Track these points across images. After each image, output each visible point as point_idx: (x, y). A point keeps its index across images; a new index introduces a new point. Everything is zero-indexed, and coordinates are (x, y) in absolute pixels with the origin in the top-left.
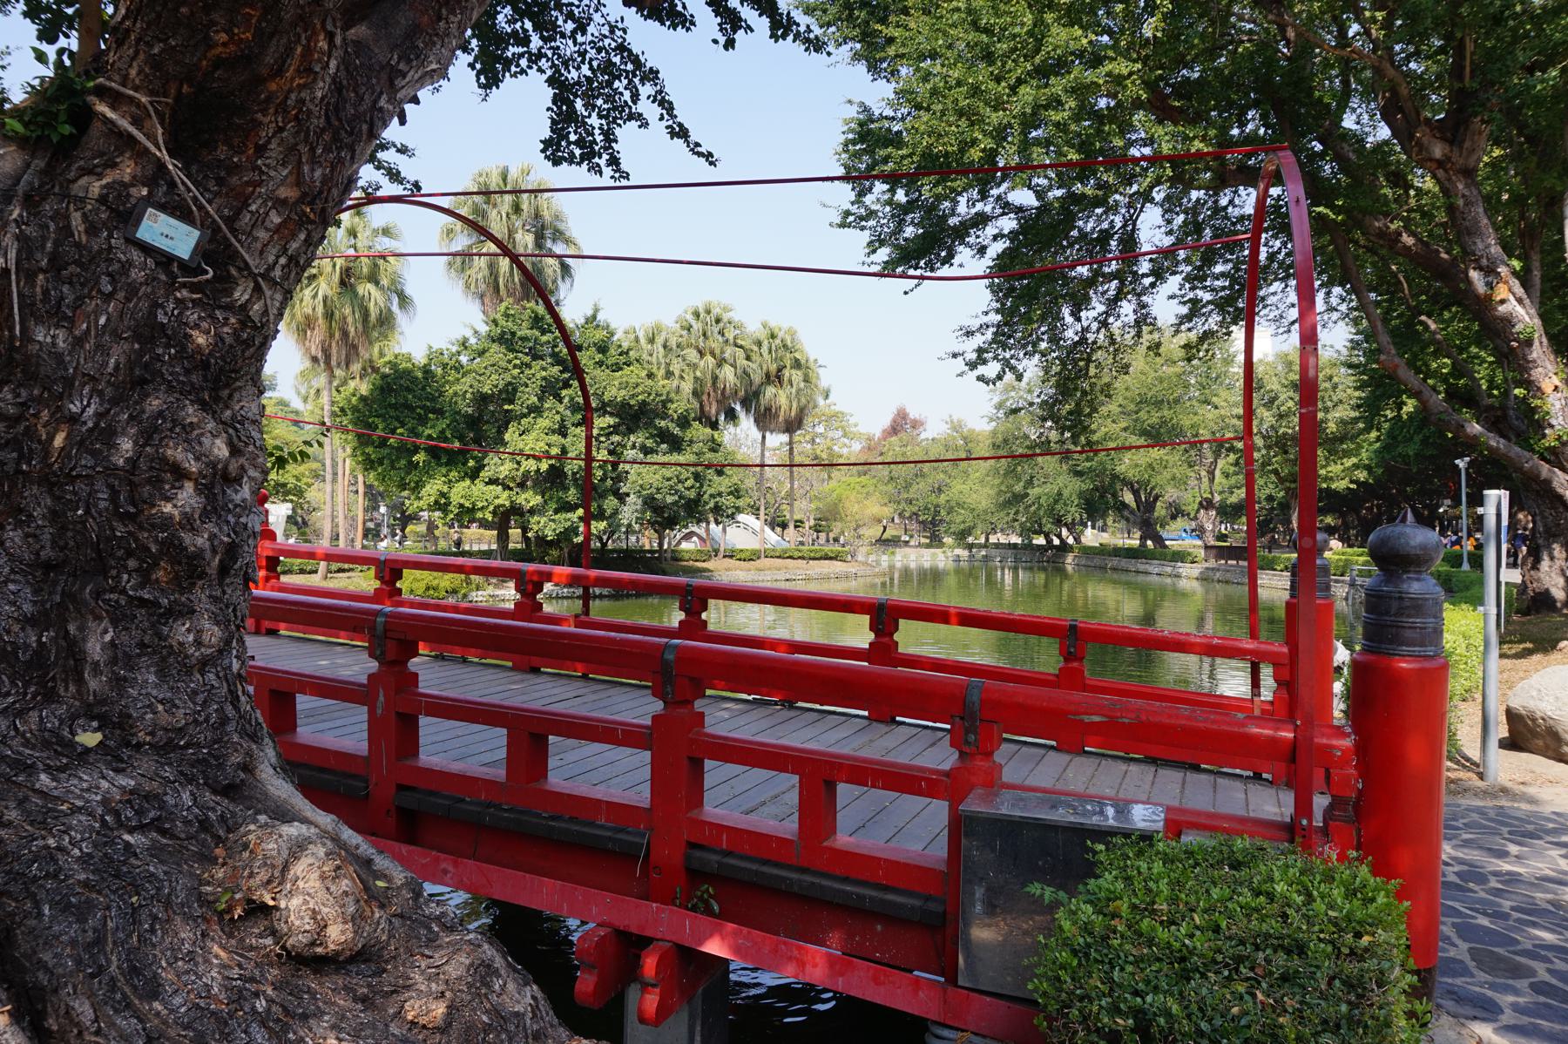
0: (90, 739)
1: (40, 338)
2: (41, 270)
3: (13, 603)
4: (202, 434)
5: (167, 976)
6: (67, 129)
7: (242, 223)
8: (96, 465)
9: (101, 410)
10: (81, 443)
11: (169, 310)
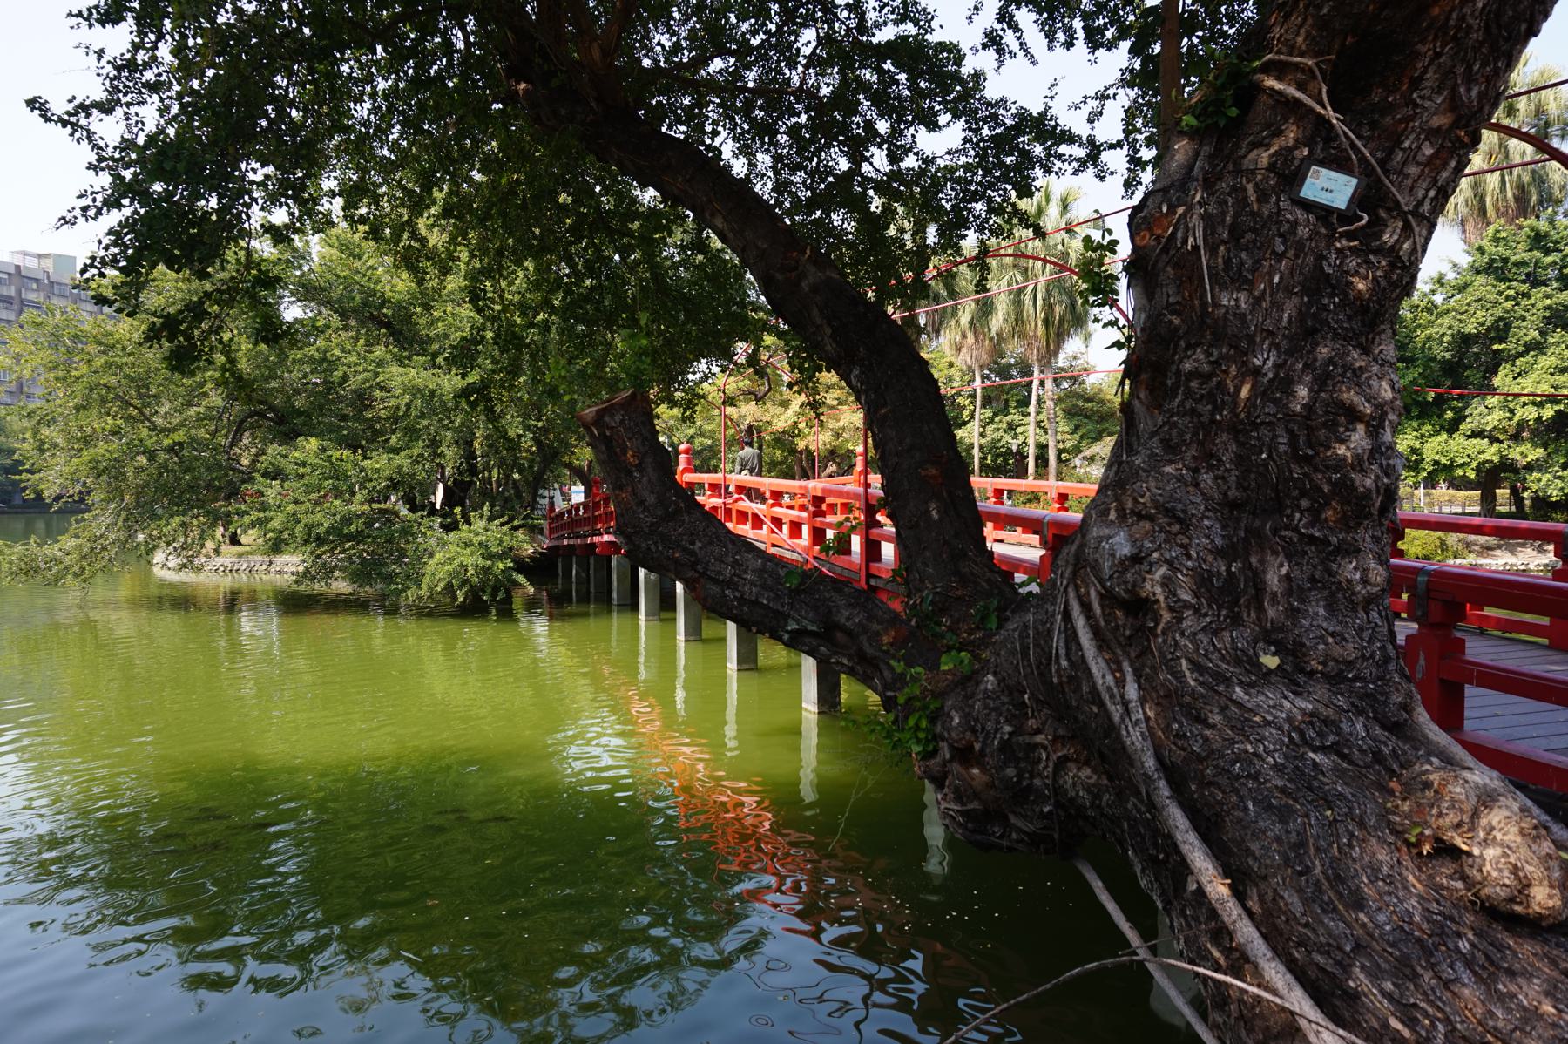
0: (1271, 661)
1: (1225, 303)
2: (1223, 242)
3: (1208, 537)
4: (1370, 377)
5: (1368, 891)
6: (1234, 112)
7: (1395, 163)
8: (1278, 412)
9: (1280, 361)
10: (1264, 393)
11: (1332, 261)
